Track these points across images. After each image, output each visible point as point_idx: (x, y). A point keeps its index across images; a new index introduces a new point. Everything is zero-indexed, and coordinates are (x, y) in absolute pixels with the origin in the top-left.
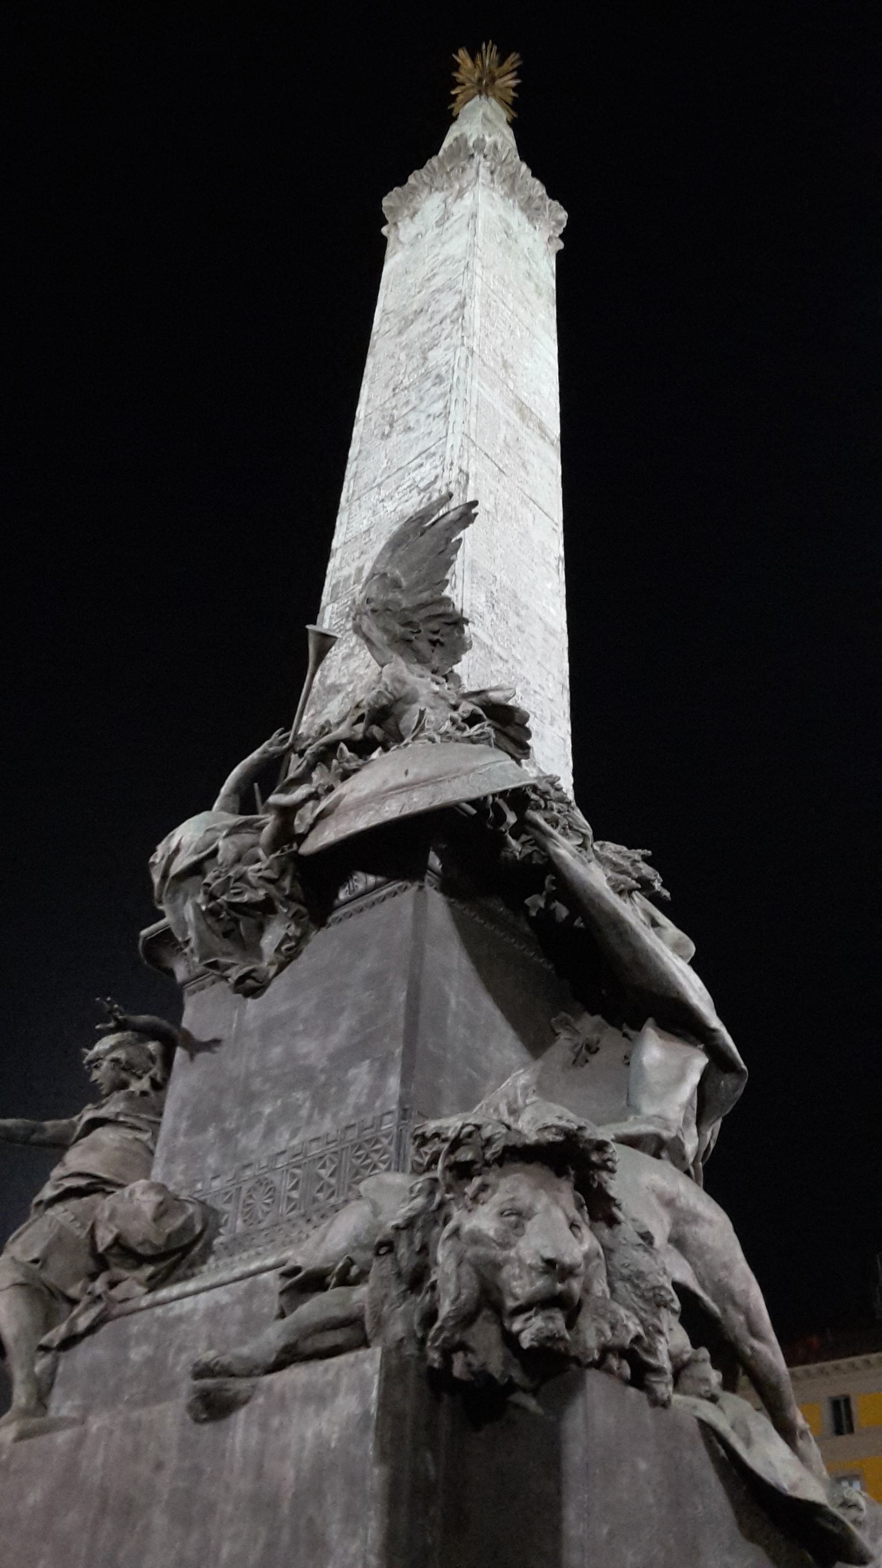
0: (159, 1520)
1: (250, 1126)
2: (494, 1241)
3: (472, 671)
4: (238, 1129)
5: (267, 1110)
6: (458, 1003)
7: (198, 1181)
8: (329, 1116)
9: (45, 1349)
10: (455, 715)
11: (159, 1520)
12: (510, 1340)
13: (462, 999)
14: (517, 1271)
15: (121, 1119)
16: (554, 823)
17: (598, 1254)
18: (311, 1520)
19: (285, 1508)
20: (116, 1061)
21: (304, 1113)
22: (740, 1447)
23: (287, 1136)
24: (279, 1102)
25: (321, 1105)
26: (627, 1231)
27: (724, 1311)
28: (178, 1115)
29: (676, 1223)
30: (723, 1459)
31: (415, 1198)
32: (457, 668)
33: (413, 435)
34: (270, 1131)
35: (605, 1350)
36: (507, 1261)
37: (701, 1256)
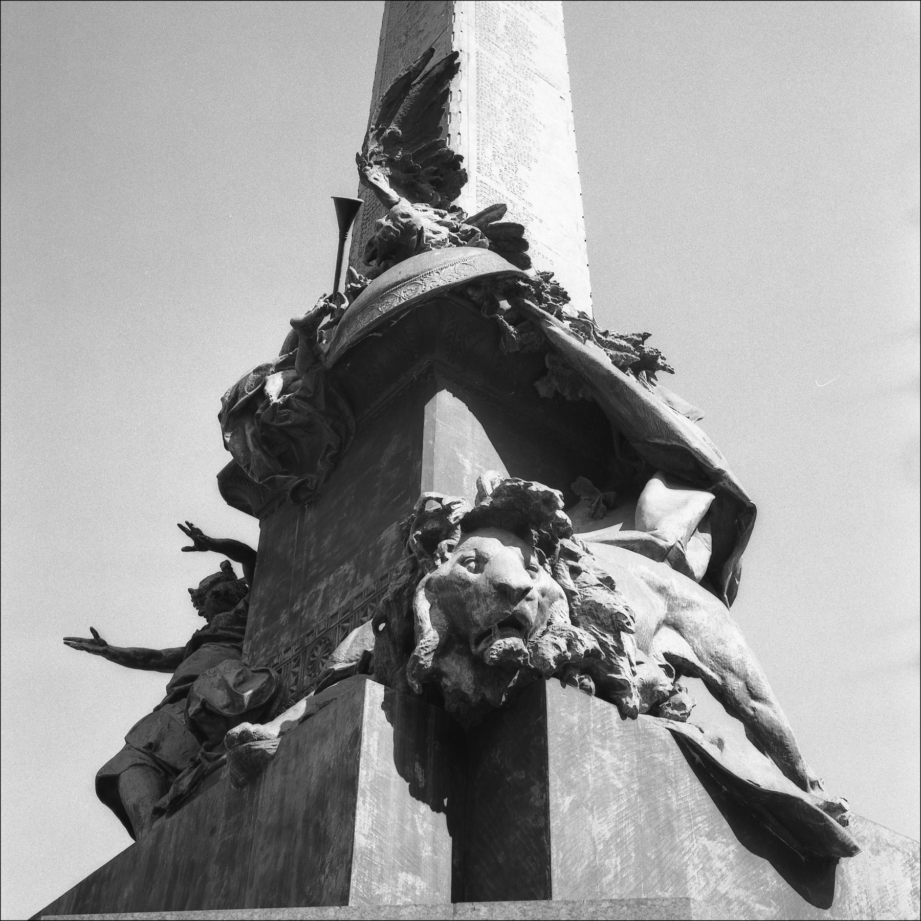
0: (213, 869)
1: (311, 603)
2: (456, 583)
3: (471, 201)
4: (301, 609)
5: (322, 586)
6: (473, 467)
7: (274, 658)
8: (368, 576)
9: (158, 812)
10: (454, 235)
11: (213, 869)
12: (478, 663)
13: (477, 465)
14: (475, 602)
15: (220, 632)
16: (550, 309)
17: (562, 597)
18: (317, 825)
19: (300, 825)
20: (216, 594)
21: (350, 579)
22: (713, 751)
23: (337, 601)
24: (331, 578)
25: (363, 569)
26: (591, 577)
27: (723, 678)
28: (257, 614)
29: (670, 609)
30: (699, 764)
31: (401, 576)
32: (459, 202)
33: (422, 36)
34: (326, 600)
35: (560, 659)
36: (469, 597)
37: (697, 635)
